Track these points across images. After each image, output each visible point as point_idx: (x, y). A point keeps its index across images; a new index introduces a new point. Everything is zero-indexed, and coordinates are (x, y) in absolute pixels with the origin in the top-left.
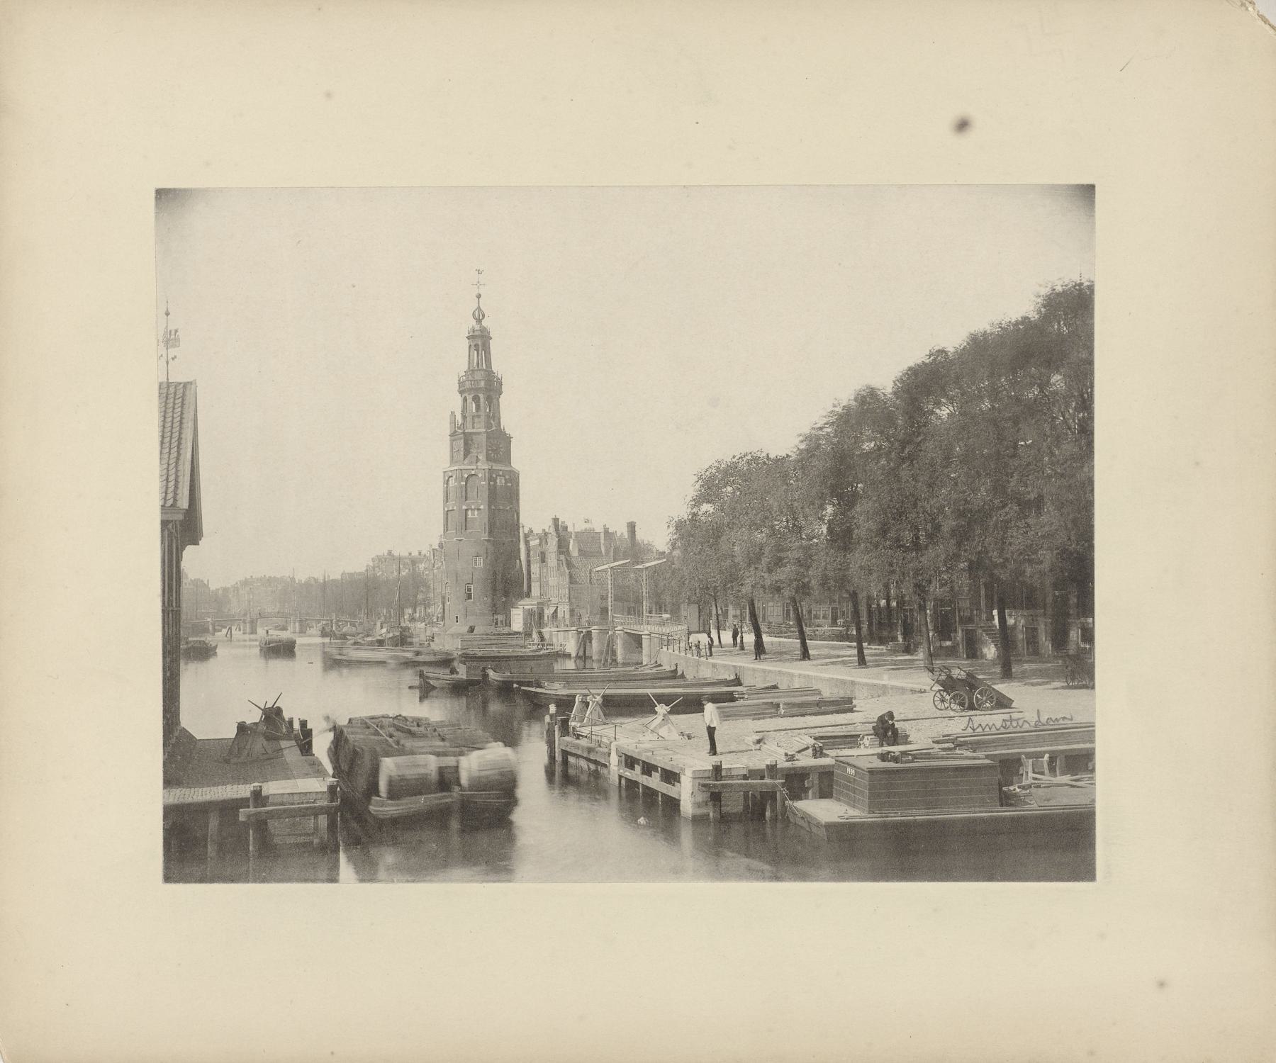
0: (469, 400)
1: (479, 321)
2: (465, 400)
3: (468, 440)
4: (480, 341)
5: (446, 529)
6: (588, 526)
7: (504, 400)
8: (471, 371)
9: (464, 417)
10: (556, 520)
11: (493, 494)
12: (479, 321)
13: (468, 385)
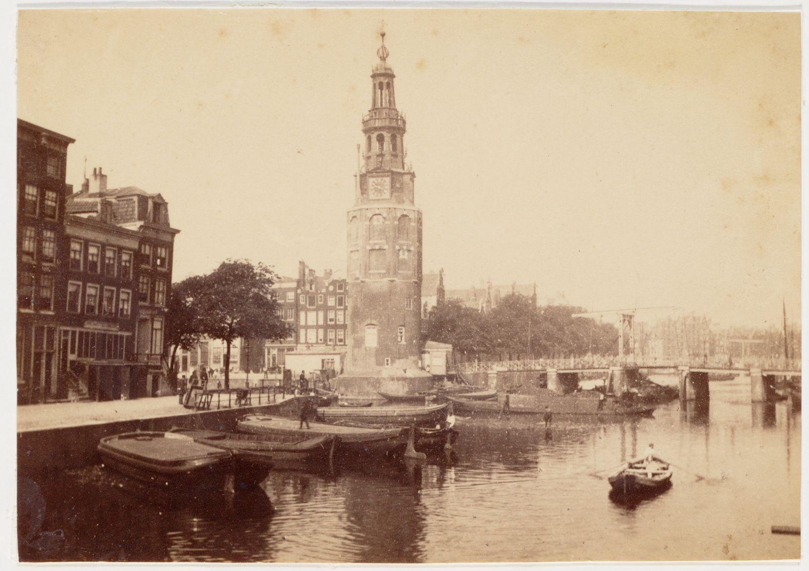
1: (383, 59)
2: (369, 138)
4: (384, 80)
7: (406, 137)
12: (383, 59)
13: (372, 124)
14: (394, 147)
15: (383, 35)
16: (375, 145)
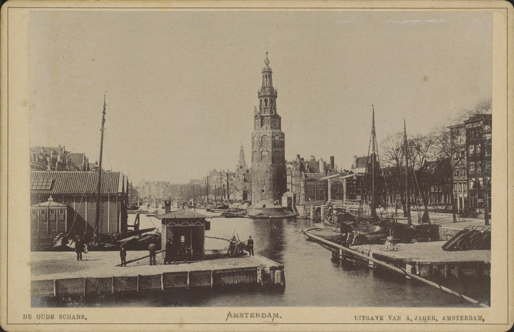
1: (267, 64)
2: (261, 101)
3: (262, 118)
4: (268, 74)
5: (253, 160)
6: (312, 158)
8: (263, 88)
9: (261, 109)
10: (299, 156)
12: (267, 64)
13: (262, 94)
15: (267, 53)
16: (264, 103)
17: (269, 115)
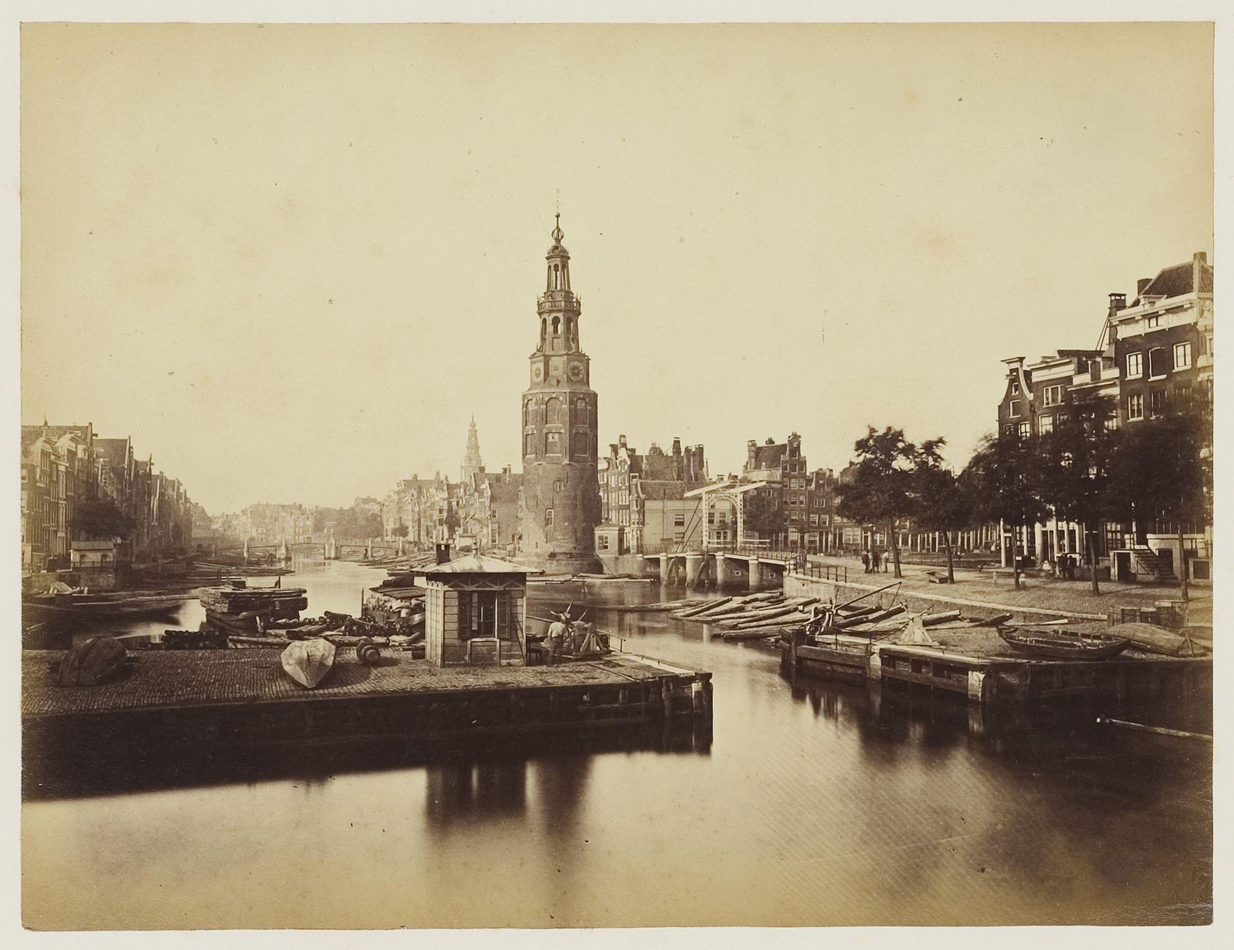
0: (549, 322)
1: (558, 240)
2: (544, 321)
8: (550, 293)
11: (574, 416)
12: (558, 240)
14: (568, 328)
16: (550, 329)
17: (563, 352)
